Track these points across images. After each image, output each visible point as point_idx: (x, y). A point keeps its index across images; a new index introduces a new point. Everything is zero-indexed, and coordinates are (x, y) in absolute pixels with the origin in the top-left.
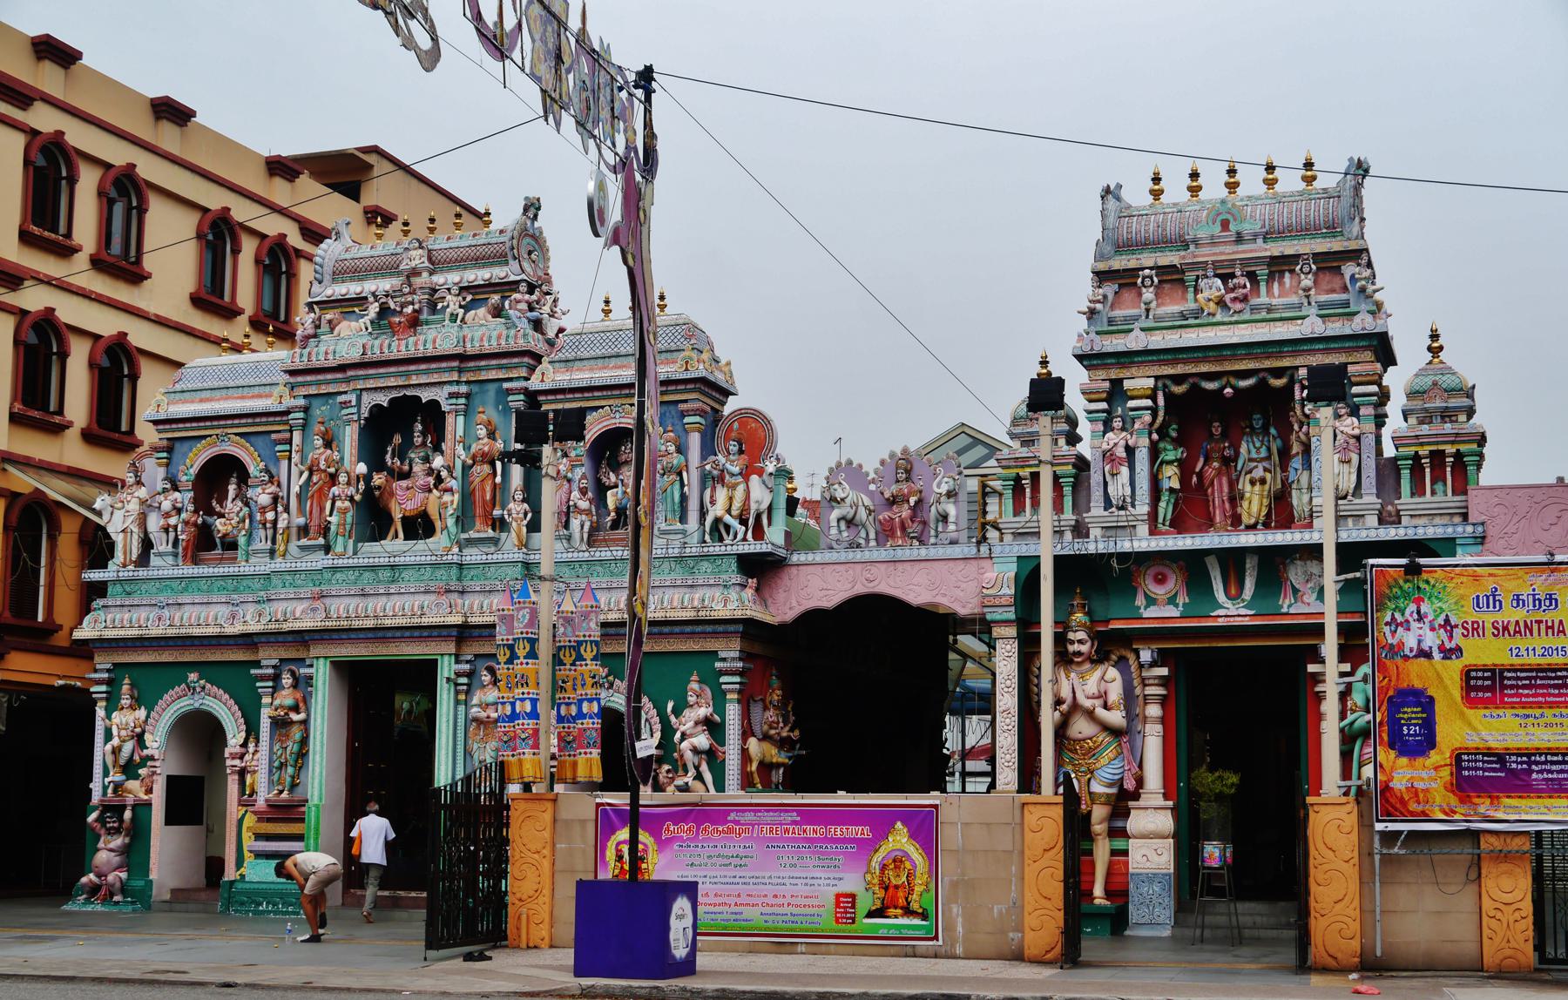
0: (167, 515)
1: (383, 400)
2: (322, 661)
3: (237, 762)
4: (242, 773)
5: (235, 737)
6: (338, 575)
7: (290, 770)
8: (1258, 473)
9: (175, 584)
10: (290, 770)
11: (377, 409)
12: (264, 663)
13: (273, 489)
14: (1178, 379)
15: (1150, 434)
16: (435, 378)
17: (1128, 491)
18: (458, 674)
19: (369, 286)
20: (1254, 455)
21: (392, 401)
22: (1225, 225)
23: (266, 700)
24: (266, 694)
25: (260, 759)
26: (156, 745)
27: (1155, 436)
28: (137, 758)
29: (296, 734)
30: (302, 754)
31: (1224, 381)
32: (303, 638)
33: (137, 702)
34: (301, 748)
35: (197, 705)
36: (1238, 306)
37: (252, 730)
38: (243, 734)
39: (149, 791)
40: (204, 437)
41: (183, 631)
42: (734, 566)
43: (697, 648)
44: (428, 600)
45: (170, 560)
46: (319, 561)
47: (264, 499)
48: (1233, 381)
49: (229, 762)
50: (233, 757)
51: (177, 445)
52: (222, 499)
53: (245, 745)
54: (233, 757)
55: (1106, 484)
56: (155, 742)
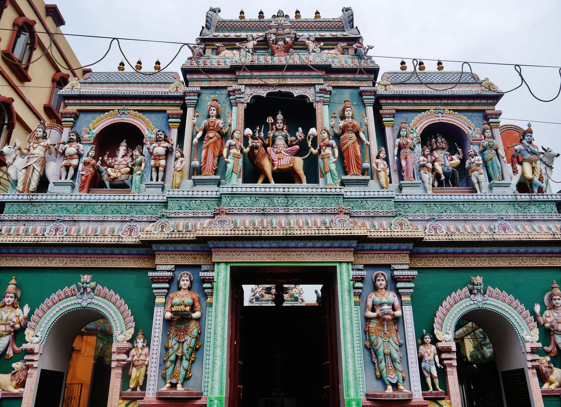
0: (71, 157)
1: (263, 93)
2: (222, 266)
3: (124, 357)
4: (126, 368)
5: (122, 333)
6: (236, 200)
7: (185, 364)
9: (71, 207)
10: (185, 364)
11: (257, 99)
12: (159, 268)
13: (166, 144)
16: (306, 81)
18: (356, 279)
21: (268, 94)
23: (160, 300)
24: (160, 295)
25: (150, 356)
26: (36, 340)
28: (10, 352)
29: (193, 328)
30: (197, 349)
32: (205, 246)
33: (19, 303)
34: (196, 343)
35: (84, 304)
37: (143, 328)
38: (132, 331)
39: (22, 384)
40: (108, 111)
41: (80, 240)
42: (555, 209)
43: (546, 264)
44: (327, 219)
45: (68, 189)
46: (211, 191)
47: (160, 150)
49: (115, 357)
50: (120, 351)
51: (82, 116)
52: (114, 155)
53: (132, 341)
54: (120, 351)
56: (35, 338)
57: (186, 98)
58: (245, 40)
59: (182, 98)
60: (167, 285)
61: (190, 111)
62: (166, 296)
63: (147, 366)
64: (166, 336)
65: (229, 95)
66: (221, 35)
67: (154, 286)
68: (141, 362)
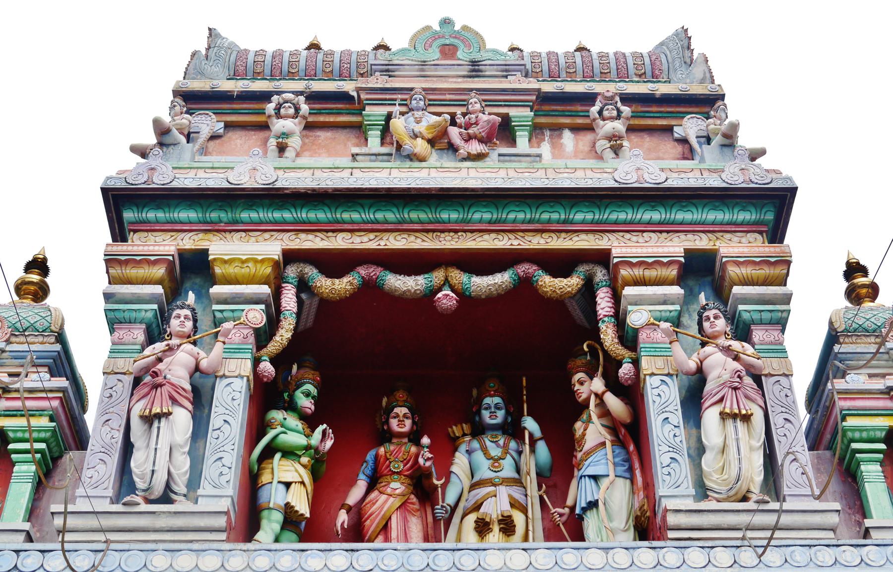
8: (497, 505)
14: (334, 263)
15: (256, 362)
17: (183, 464)
20: (485, 471)
22: (448, 51)
27: (267, 367)
31: (438, 276)
36: (475, 147)
48: (458, 277)
55: (127, 448)
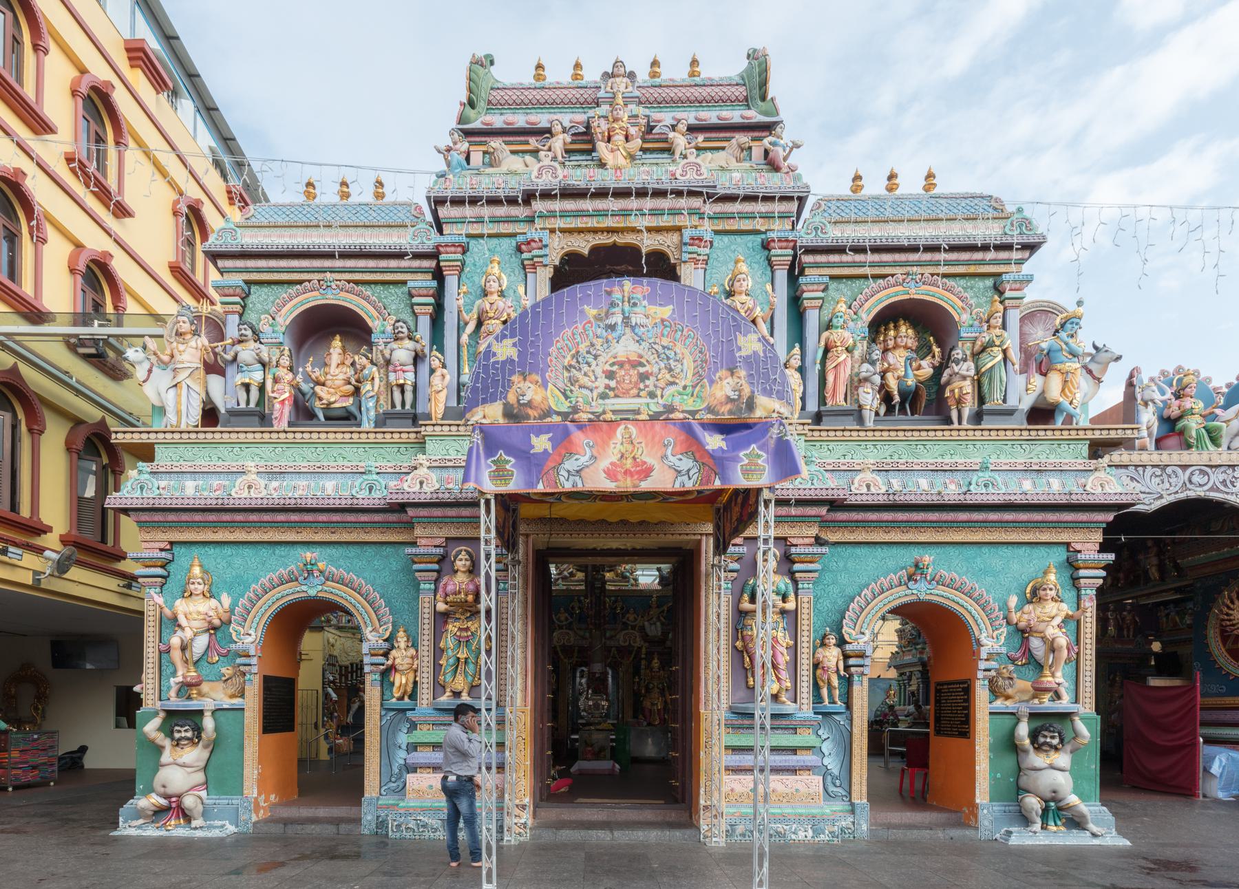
3: (381, 659)
19: (542, 119)
57: (442, 257)
58: (546, 132)
59: (434, 255)
60: (436, 567)
61: (451, 282)
62: (437, 581)
63: (416, 671)
64: (438, 634)
65: (519, 249)
66: (497, 121)
67: (416, 567)
68: (406, 667)
